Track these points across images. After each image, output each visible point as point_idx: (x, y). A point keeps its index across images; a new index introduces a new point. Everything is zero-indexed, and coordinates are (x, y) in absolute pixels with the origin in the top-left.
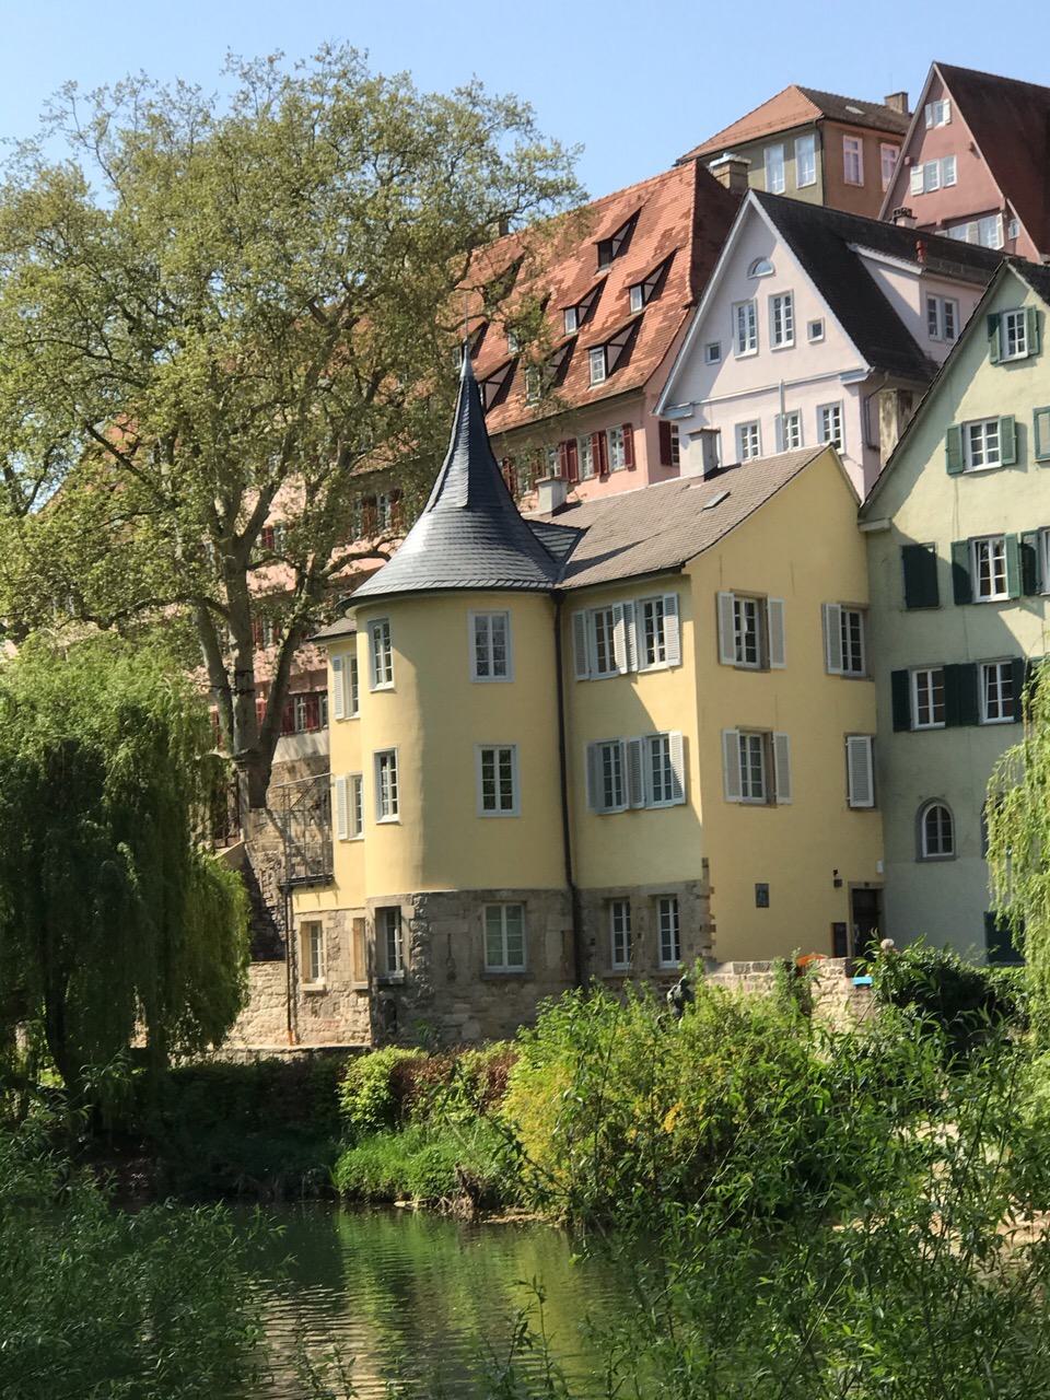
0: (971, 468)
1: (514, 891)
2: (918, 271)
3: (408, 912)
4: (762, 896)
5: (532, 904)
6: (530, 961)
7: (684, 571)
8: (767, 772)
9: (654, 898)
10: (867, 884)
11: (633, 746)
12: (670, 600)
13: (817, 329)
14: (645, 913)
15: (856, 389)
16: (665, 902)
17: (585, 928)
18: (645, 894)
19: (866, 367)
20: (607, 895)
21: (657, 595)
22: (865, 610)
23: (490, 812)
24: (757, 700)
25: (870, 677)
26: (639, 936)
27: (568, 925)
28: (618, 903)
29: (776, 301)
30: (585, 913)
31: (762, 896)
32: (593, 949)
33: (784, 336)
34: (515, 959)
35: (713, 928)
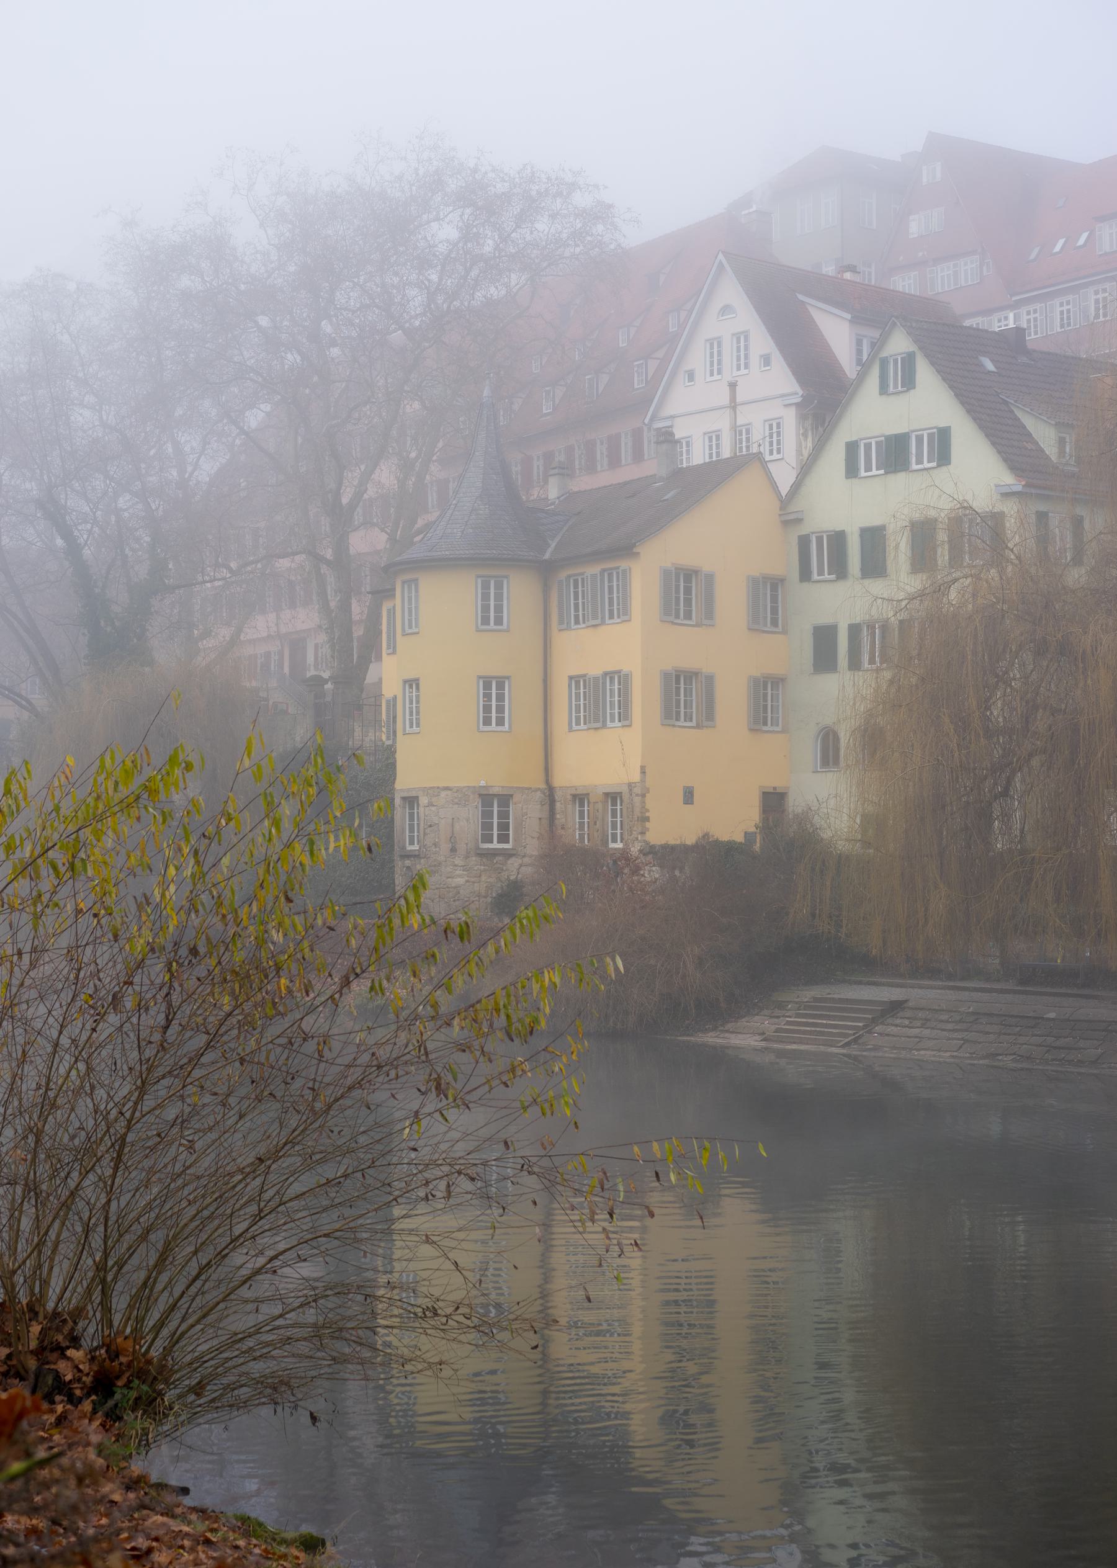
0: (863, 474)
2: (849, 316)
3: (424, 800)
4: (689, 796)
5: (517, 798)
6: (515, 840)
7: (635, 550)
8: (697, 703)
9: (607, 795)
10: (775, 788)
11: (596, 679)
12: (624, 571)
13: (766, 360)
14: (600, 806)
15: (793, 409)
16: (613, 797)
17: (558, 816)
19: (801, 392)
20: (574, 792)
21: (617, 565)
22: (782, 580)
24: (687, 648)
25: (785, 632)
26: (595, 823)
28: (580, 798)
29: (737, 336)
30: (558, 805)
31: (689, 796)
34: (504, 838)
35: (647, 819)
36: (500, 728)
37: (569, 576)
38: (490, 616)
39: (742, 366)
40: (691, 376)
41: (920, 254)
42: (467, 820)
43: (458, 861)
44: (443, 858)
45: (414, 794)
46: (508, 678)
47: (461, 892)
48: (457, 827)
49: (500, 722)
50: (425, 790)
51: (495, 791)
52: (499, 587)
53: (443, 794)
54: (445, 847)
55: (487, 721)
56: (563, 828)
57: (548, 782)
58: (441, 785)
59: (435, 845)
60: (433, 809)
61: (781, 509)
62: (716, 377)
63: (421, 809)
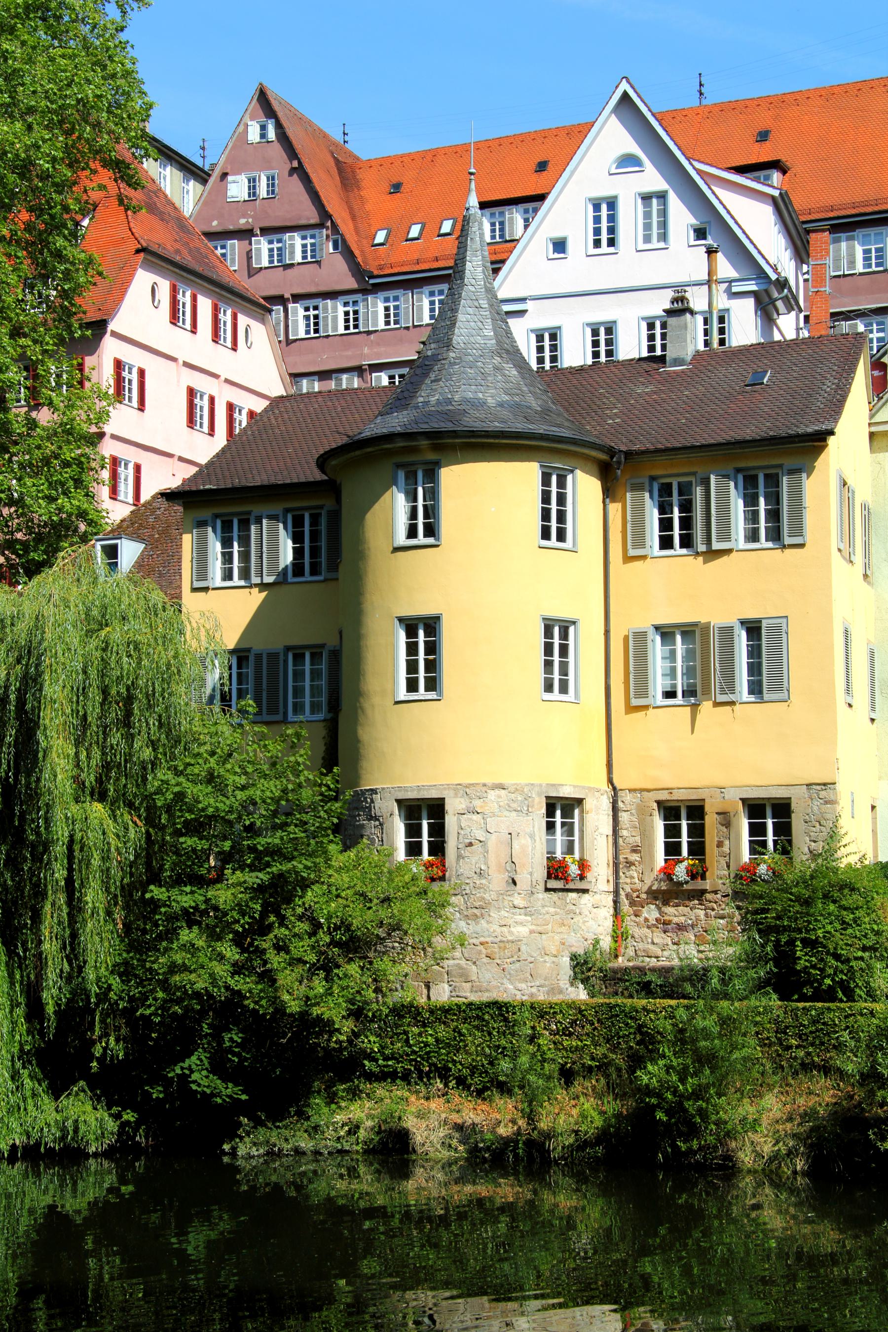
1: (574, 786)
3: (453, 806)
18: (734, 796)
20: (664, 796)
23: (548, 696)
27: (610, 832)
29: (646, 198)
32: (635, 857)
33: (604, 242)
36: (563, 697)
37: (653, 479)
38: (553, 525)
39: (604, 242)
40: (560, 246)
41: (243, 221)
42: (532, 836)
43: (519, 901)
44: (494, 896)
45: (434, 794)
46: (574, 623)
47: (523, 948)
48: (516, 846)
49: (564, 689)
50: (464, 789)
51: (567, 792)
52: (562, 484)
53: (492, 795)
54: (497, 880)
55: (549, 688)
56: (634, 851)
57: (610, 781)
58: (489, 781)
59: (480, 874)
60: (475, 817)
61: (872, 416)
62: (604, 248)
63: (451, 821)
